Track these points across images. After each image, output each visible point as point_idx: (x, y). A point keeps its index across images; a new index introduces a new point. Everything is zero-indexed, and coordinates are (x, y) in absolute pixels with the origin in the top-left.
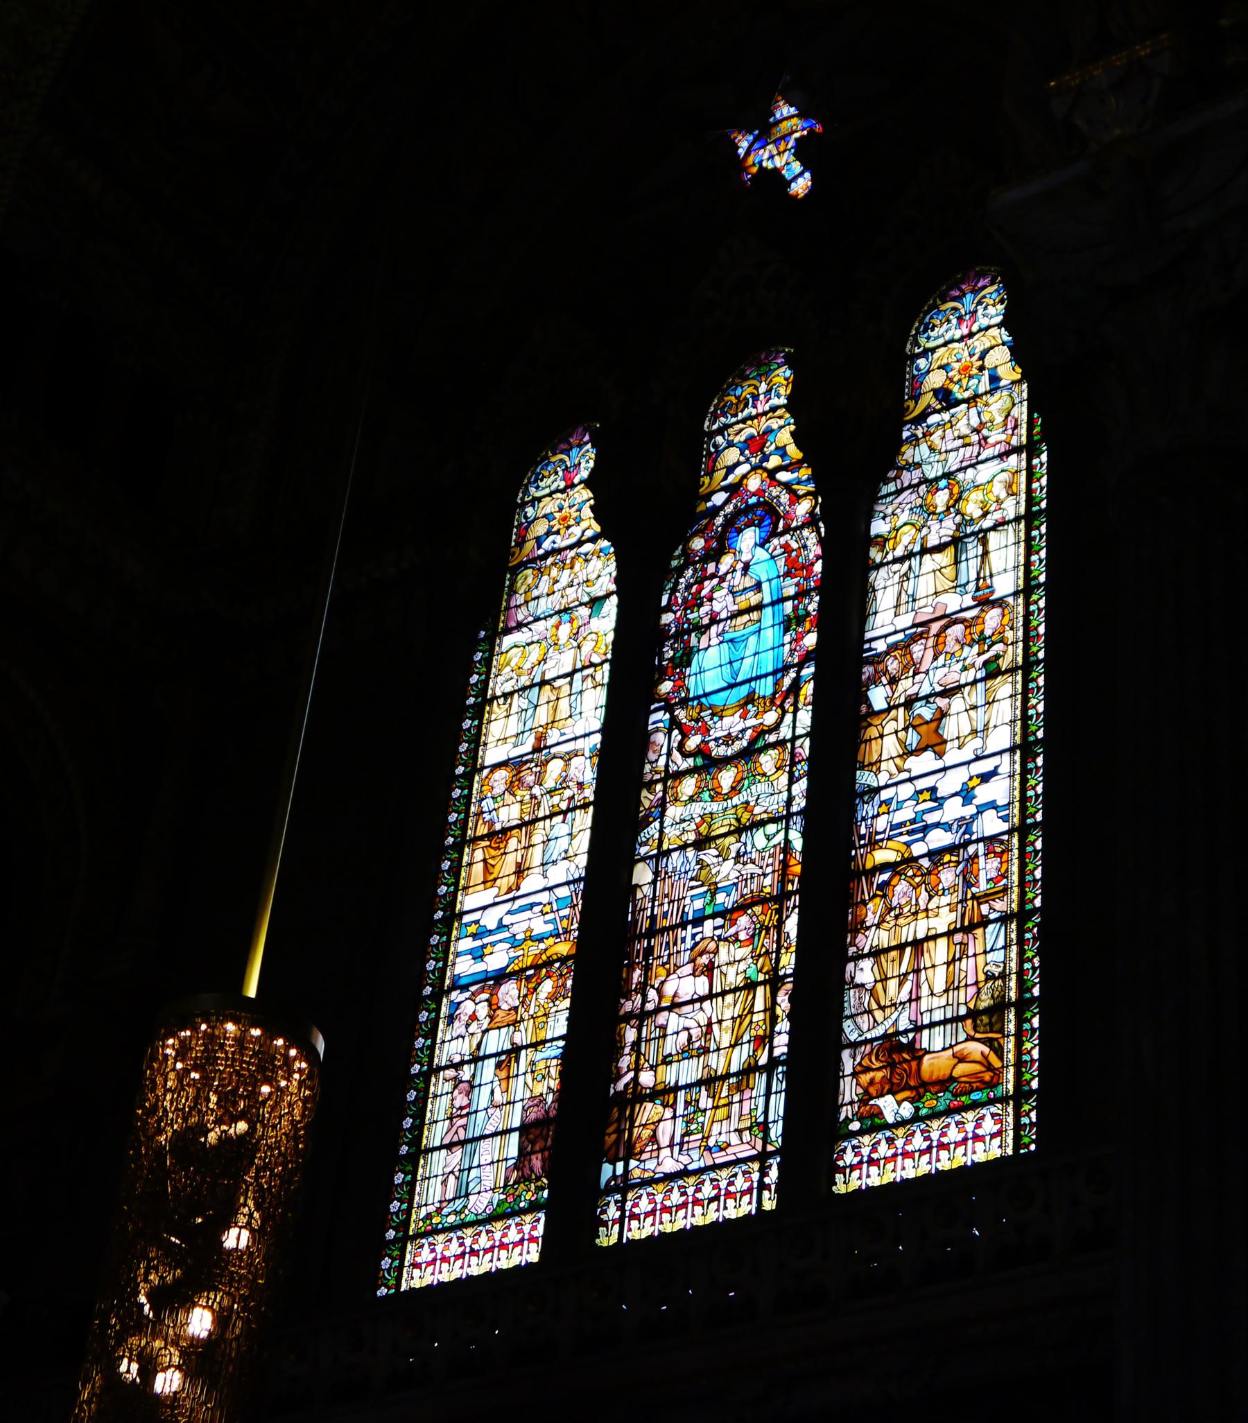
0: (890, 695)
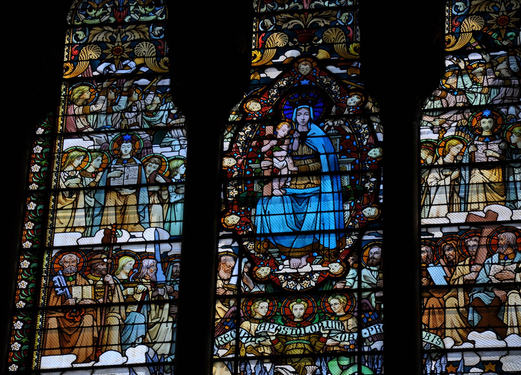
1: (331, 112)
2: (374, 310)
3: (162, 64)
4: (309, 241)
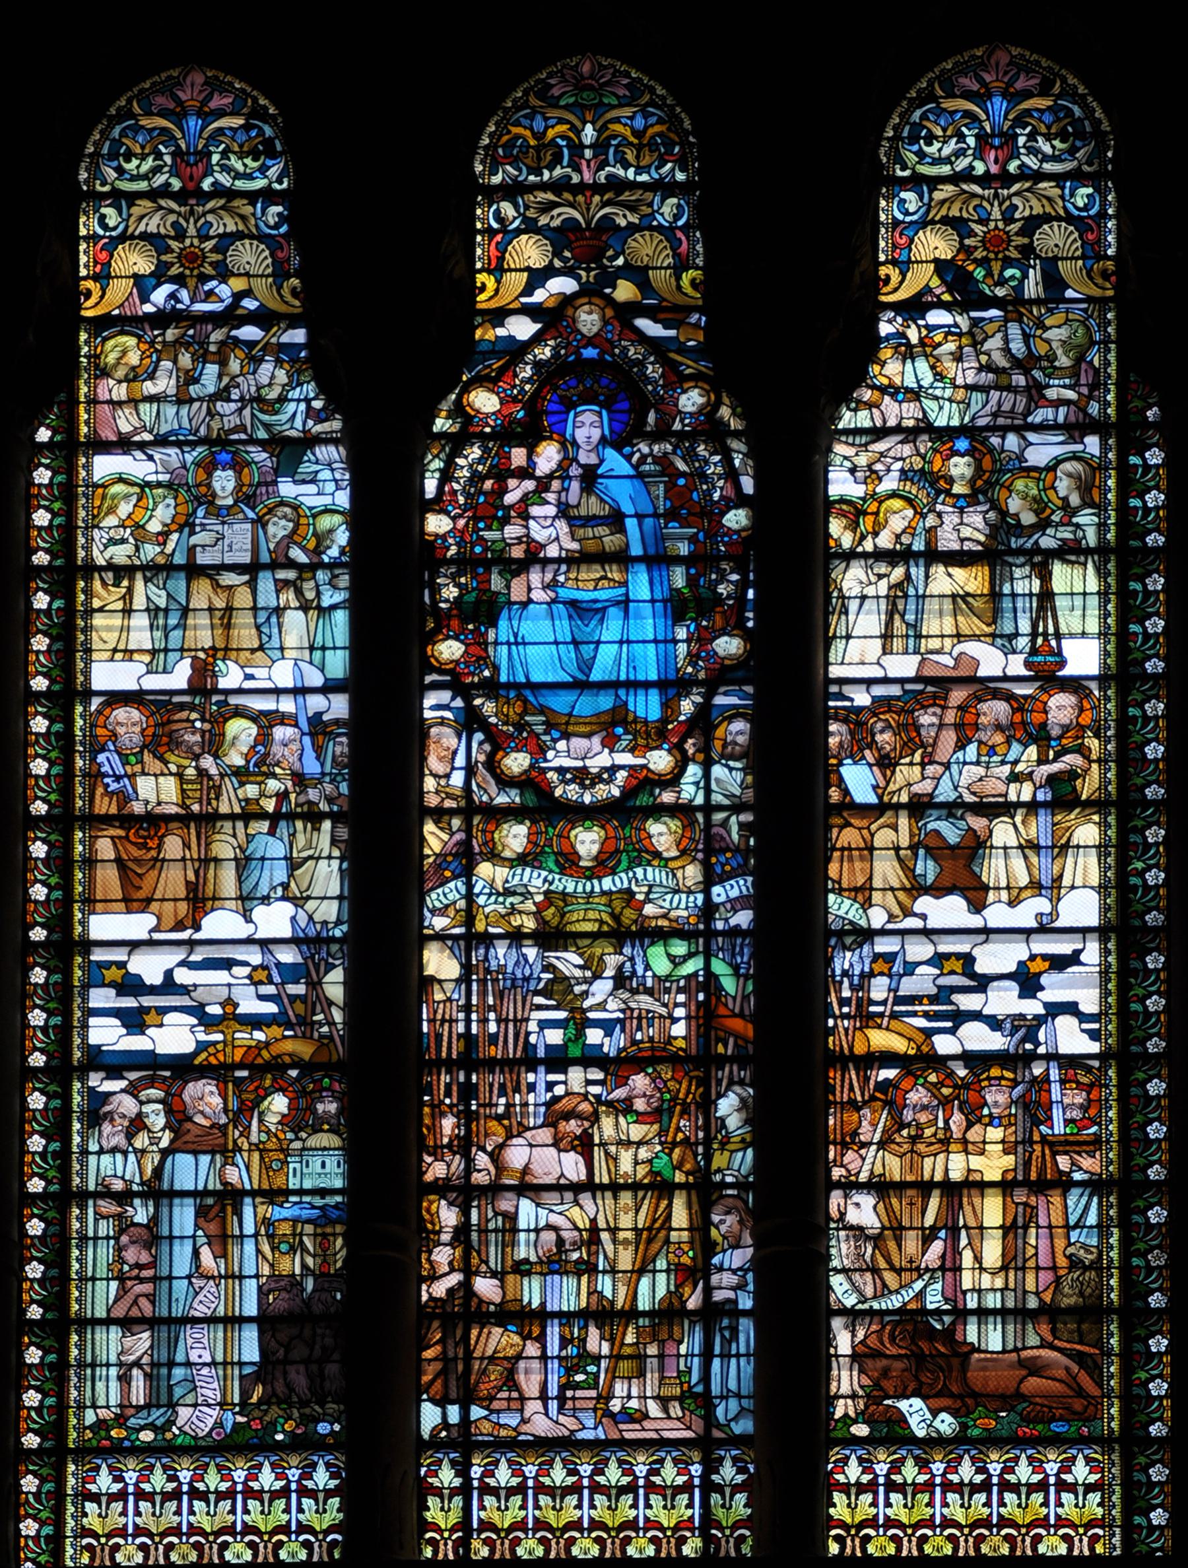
0: (882, 784)
1: (645, 423)
2: (737, 850)
3: (286, 292)
4: (605, 702)
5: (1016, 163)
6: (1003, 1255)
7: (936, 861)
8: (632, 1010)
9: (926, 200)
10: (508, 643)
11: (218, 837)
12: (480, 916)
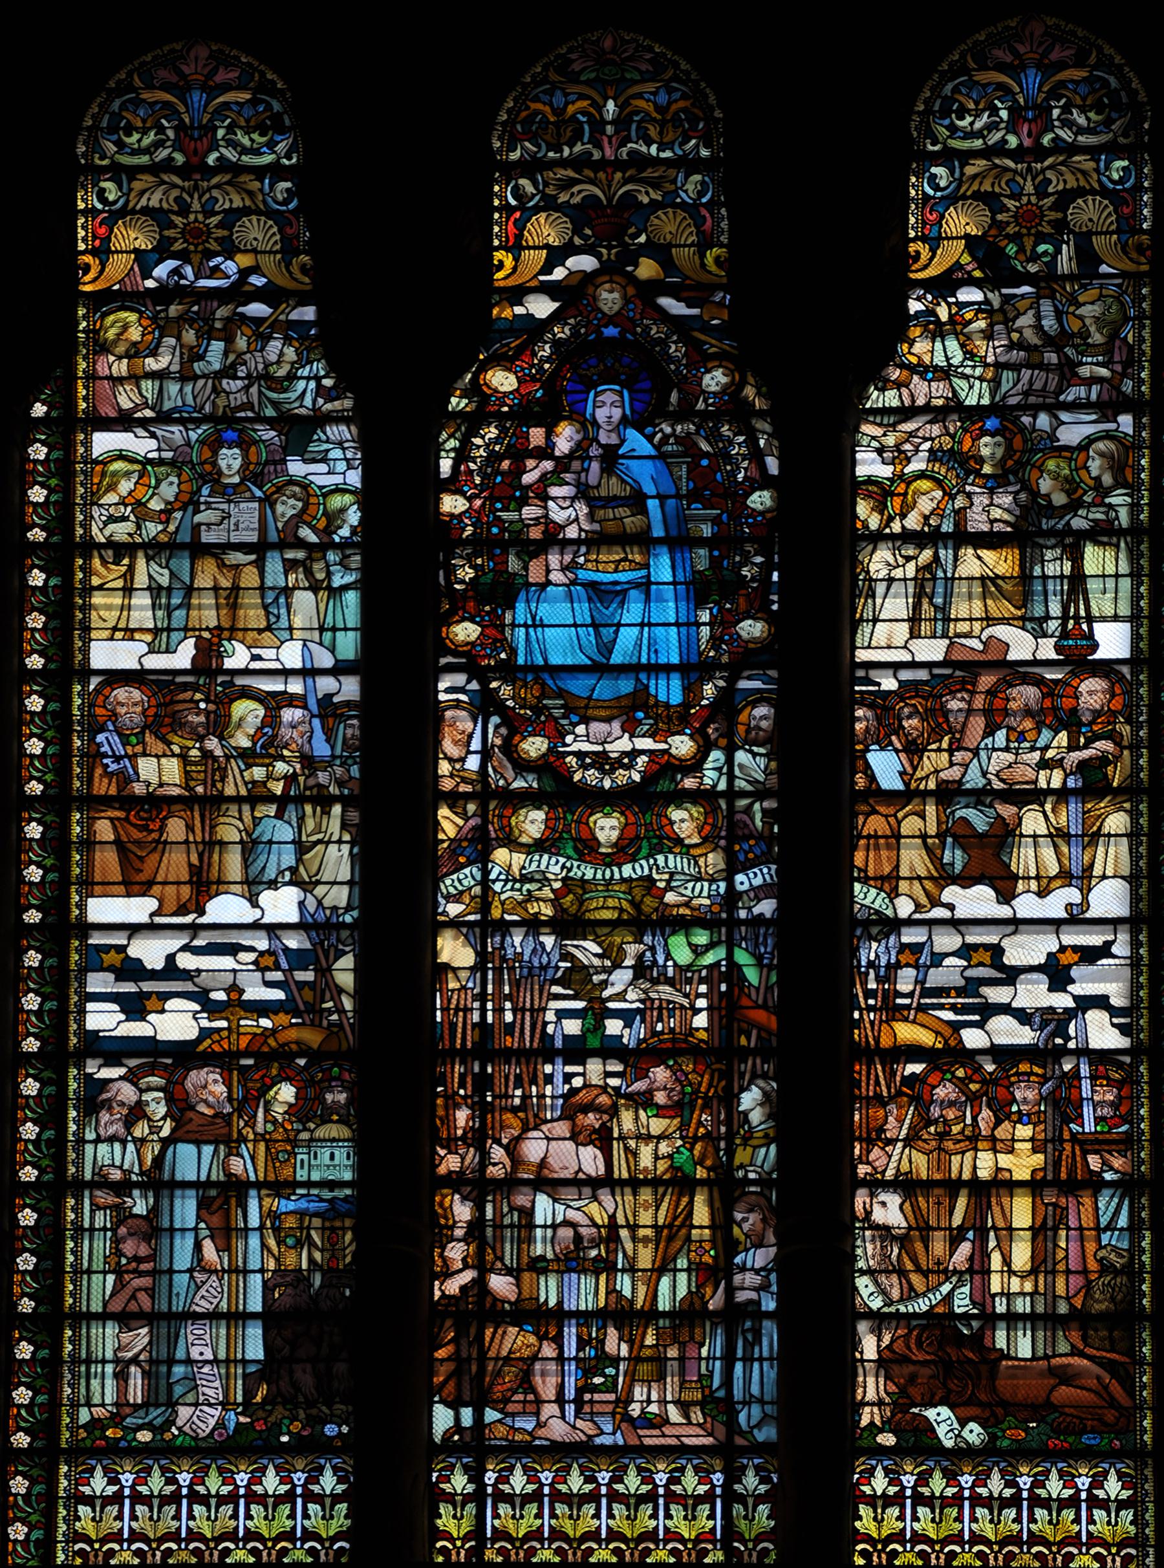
0: (909, 770)
1: (668, 402)
2: (760, 837)
3: (295, 269)
4: (626, 686)
5: (1050, 136)
6: (1033, 1257)
7: (964, 851)
8: (653, 1000)
9: (957, 175)
10: (526, 625)
11: (222, 820)
12: (496, 903)
